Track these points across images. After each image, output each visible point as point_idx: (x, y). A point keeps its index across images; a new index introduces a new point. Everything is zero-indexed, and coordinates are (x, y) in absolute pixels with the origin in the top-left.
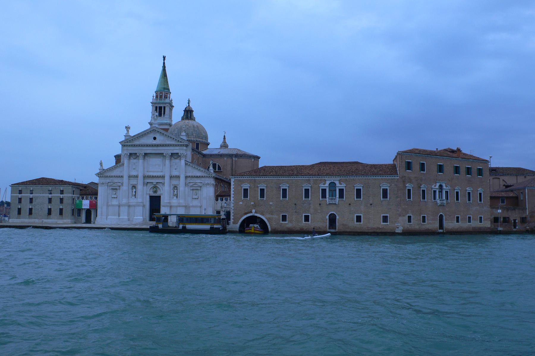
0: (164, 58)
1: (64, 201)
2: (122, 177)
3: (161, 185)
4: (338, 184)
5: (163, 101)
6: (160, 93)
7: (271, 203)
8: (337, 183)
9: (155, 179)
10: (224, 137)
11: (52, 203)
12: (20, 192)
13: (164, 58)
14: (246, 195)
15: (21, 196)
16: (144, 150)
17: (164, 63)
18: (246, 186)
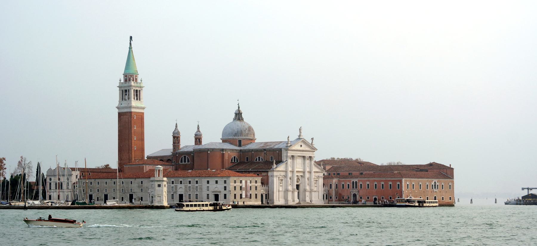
0: (131, 38)
1: (258, 188)
2: (286, 172)
3: (301, 177)
4: (437, 183)
5: (138, 85)
6: (136, 76)
7: (416, 191)
8: (436, 182)
9: (299, 173)
10: (198, 126)
11: (252, 190)
12: (235, 182)
13: (131, 38)
14: (408, 188)
15: (236, 185)
16: (297, 153)
17: (130, 44)
18: (408, 183)
